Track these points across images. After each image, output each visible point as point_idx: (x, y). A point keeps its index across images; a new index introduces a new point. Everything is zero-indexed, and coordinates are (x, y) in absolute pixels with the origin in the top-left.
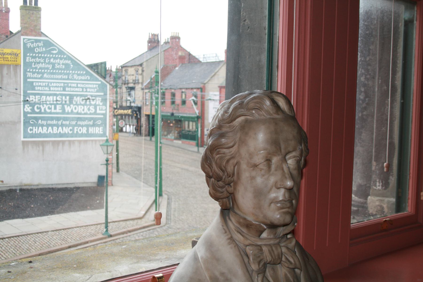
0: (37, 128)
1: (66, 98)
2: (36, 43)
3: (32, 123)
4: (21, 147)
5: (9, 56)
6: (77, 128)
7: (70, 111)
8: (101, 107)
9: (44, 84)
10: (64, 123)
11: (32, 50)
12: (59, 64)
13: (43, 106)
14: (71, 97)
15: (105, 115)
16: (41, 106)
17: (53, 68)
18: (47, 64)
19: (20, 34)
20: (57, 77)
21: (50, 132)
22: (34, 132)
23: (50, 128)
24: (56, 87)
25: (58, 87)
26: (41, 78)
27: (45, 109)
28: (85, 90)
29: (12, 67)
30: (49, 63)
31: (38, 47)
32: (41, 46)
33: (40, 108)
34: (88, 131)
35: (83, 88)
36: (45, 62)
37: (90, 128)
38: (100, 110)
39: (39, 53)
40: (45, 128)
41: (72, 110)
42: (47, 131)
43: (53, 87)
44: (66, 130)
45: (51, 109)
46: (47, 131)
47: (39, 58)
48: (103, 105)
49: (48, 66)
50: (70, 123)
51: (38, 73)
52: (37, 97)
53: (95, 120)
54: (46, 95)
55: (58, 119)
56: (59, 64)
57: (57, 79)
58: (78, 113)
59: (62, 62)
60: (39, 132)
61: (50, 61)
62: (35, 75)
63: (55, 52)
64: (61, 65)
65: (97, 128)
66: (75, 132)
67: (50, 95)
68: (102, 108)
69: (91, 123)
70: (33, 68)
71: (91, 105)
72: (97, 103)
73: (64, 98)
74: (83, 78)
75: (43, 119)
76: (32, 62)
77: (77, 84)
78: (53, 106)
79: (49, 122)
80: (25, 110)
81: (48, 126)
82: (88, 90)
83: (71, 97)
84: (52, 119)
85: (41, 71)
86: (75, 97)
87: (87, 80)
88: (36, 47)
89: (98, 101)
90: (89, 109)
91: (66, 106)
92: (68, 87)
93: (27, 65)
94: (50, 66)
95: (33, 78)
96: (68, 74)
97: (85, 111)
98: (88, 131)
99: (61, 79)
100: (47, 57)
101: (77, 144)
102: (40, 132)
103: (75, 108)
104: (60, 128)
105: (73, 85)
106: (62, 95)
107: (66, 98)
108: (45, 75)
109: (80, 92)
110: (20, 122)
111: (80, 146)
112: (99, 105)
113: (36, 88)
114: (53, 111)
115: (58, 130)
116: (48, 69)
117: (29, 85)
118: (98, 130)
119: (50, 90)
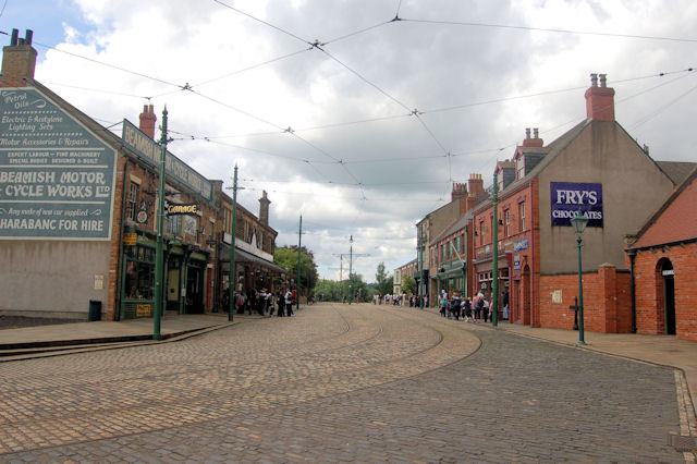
10: (45, 212)
14: (59, 172)
15: (108, 200)
20: (42, 142)
26: (20, 146)
27: (19, 192)
28: (79, 161)
30: (32, 123)
35: (76, 158)
44: (47, 224)
55: (36, 207)
57: (41, 146)
58: (66, 198)
62: (12, 142)
63: (41, 106)
67: (28, 170)
71: (87, 184)
73: (47, 174)
74: (78, 143)
75: (16, 206)
77: (69, 152)
78: (31, 187)
81: (21, 217)
83: (59, 172)
84: (28, 206)
87: (85, 146)
89: (99, 177)
90: (83, 192)
91: (49, 187)
92: (55, 157)
94: (33, 128)
96: (57, 138)
98: (79, 226)
99: (48, 146)
101: (61, 246)
104: (39, 221)
105: (63, 154)
106: (45, 170)
108: (25, 142)
111: (65, 250)
114: (31, 194)
116: (29, 131)
118: (96, 226)
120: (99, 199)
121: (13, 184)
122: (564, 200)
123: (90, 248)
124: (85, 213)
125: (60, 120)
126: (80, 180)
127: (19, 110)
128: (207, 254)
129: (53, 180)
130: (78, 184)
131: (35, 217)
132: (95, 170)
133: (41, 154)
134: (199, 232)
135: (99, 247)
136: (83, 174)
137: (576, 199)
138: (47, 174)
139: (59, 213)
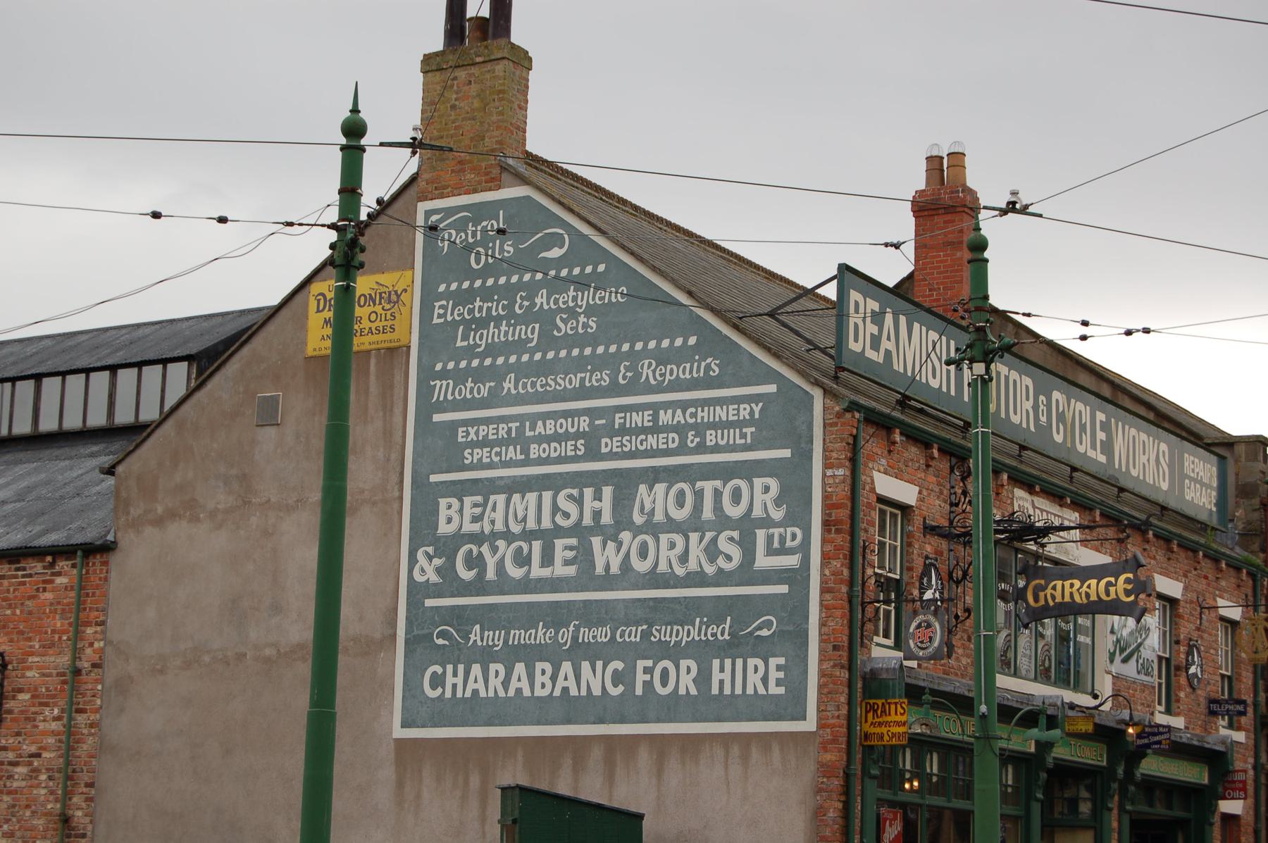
1: (598, 497)
3: (440, 642)
4: (387, 773)
6: (649, 663)
7: (615, 569)
8: (776, 532)
10: (586, 635)
12: (572, 313)
13: (494, 550)
14: (624, 484)
15: (797, 578)
19: (413, 191)
22: (448, 694)
24: (556, 438)
25: (566, 437)
27: (500, 565)
28: (692, 440)
29: (373, 362)
30: (530, 316)
33: (475, 562)
35: (680, 429)
36: (511, 314)
37: (716, 663)
38: (770, 552)
41: (626, 564)
42: (506, 684)
43: (540, 439)
44: (595, 680)
46: (506, 684)
47: (486, 294)
48: (789, 521)
50: (613, 637)
51: (479, 376)
52: (468, 501)
54: (522, 486)
55: (556, 616)
56: (572, 313)
58: (655, 579)
60: (468, 694)
61: (533, 304)
62: (468, 389)
63: (556, 253)
64: (582, 319)
65: (752, 662)
66: (639, 691)
67: (522, 486)
68: (782, 539)
69: (723, 632)
70: (457, 355)
71: (723, 522)
72: (757, 512)
73: (589, 492)
74: (685, 372)
76: (455, 324)
77: (655, 408)
78: (537, 546)
80: (418, 577)
81: (511, 655)
83: (624, 484)
85: (493, 365)
86: (643, 488)
87: (708, 383)
88: (476, 244)
89: (763, 496)
90: (712, 552)
91: (596, 541)
94: (532, 333)
97: (692, 565)
98: (703, 679)
99: (583, 392)
100: (520, 286)
101: (644, 757)
103: (643, 554)
104: (567, 667)
105: (637, 419)
107: (598, 497)
108: (508, 385)
109: (667, 453)
110: (394, 636)
111: (660, 772)
112: (767, 522)
113: (469, 457)
114: (537, 572)
115: (554, 679)
116: (519, 346)
117: (443, 447)
118: (759, 676)
119: (527, 462)
120: (768, 577)
121: (477, 539)
123: (745, 758)
124: (723, 632)
125: (614, 296)
126: (698, 507)
127: (485, 272)
128: (1216, 760)
129: (606, 518)
130: (695, 524)
132: (749, 471)
133: (566, 425)
134: (1170, 667)
136: (708, 486)
138: (589, 492)
139: (633, 635)
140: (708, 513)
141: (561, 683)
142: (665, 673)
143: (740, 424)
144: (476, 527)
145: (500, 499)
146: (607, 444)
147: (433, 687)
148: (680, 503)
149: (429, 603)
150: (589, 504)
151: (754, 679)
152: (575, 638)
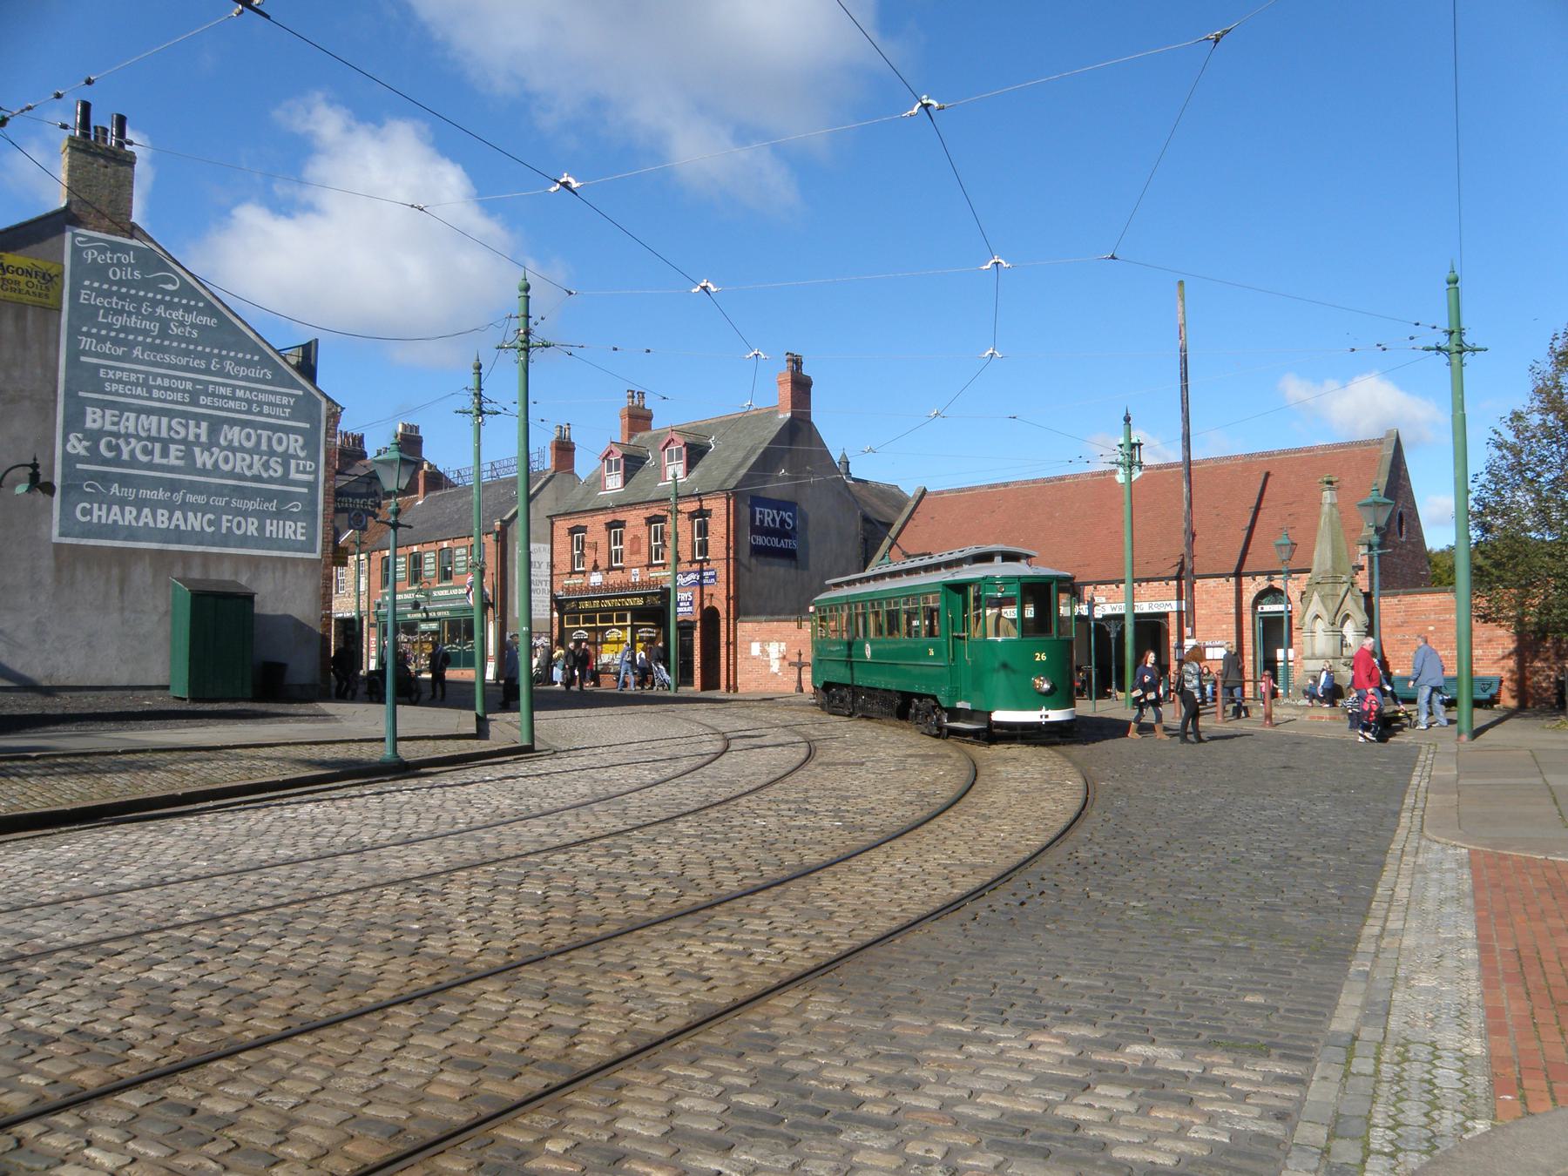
0: (104, 507)
1: (198, 426)
2: (113, 252)
4: (47, 562)
5: (23, 279)
7: (209, 466)
9: (133, 377)
10: (191, 498)
11: (99, 271)
15: (312, 486)
16: (121, 442)
17: (164, 333)
18: (144, 318)
20: (174, 360)
21: (146, 524)
22: (95, 520)
23: (146, 511)
25: (177, 390)
26: (125, 358)
27: (132, 452)
28: (255, 408)
30: (151, 317)
31: (119, 264)
32: (129, 264)
33: (117, 448)
34: (261, 528)
35: (249, 402)
38: (298, 471)
39: (120, 283)
40: (130, 512)
42: (137, 518)
43: (160, 388)
44: (196, 522)
45: (151, 453)
46: (137, 518)
47: (122, 297)
49: (146, 324)
51: (116, 342)
52: (108, 412)
53: (285, 497)
54: (140, 411)
55: (173, 486)
56: (182, 324)
58: (232, 475)
59: (189, 319)
63: (170, 287)
66: (224, 531)
67: (150, 412)
70: (100, 326)
72: (291, 451)
75: (125, 481)
76: (97, 308)
77: (234, 387)
78: (158, 446)
79: (145, 493)
80: (69, 448)
81: (140, 504)
82: (266, 409)
83: (215, 425)
84: (156, 484)
87: (264, 381)
89: (295, 443)
90: (266, 466)
91: (197, 450)
92: (207, 395)
93: (83, 314)
94: (155, 327)
95: (97, 355)
96: (208, 357)
97: (255, 471)
98: (261, 528)
100: (145, 298)
102: (115, 522)
103: (226, 461)
104: (178, 514)
105: (222, 390)
107: (198, 426)
108: (137, 352)
112: (296, 457)
114: (157, 459)
115: (170, 519)
116: (146, 333)
117: (86, 377)
118: (293, 530)
119: (151, 398)
121: (117, 435)
122: (762, 521)
126: (259, 442)
129: (204, 439)
130: (256, 450)
131: (171, 507)
132: (288, 430)
133: (178, 384)
135: (301, 569)
136: (265, 434)
137: (774, 520)
140: (264, 447)
141: (174, 522)
142: (239, 524)
143: (283, 406)
144: (115, 428)
145: (132, 416)
146: (203, 400)
147: (84, 515)
148: (248, 437)
149: (79, 466)
150: (192, 429)
151: (289, 532)
152: (184, 499)
